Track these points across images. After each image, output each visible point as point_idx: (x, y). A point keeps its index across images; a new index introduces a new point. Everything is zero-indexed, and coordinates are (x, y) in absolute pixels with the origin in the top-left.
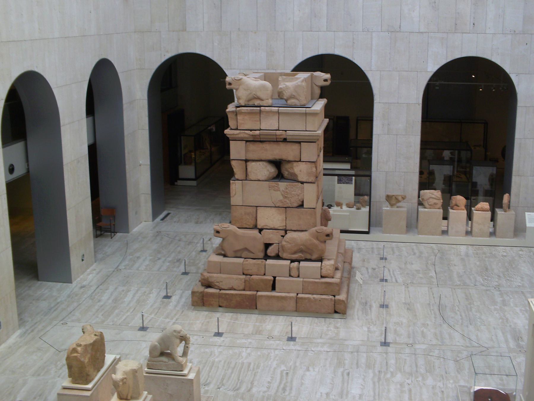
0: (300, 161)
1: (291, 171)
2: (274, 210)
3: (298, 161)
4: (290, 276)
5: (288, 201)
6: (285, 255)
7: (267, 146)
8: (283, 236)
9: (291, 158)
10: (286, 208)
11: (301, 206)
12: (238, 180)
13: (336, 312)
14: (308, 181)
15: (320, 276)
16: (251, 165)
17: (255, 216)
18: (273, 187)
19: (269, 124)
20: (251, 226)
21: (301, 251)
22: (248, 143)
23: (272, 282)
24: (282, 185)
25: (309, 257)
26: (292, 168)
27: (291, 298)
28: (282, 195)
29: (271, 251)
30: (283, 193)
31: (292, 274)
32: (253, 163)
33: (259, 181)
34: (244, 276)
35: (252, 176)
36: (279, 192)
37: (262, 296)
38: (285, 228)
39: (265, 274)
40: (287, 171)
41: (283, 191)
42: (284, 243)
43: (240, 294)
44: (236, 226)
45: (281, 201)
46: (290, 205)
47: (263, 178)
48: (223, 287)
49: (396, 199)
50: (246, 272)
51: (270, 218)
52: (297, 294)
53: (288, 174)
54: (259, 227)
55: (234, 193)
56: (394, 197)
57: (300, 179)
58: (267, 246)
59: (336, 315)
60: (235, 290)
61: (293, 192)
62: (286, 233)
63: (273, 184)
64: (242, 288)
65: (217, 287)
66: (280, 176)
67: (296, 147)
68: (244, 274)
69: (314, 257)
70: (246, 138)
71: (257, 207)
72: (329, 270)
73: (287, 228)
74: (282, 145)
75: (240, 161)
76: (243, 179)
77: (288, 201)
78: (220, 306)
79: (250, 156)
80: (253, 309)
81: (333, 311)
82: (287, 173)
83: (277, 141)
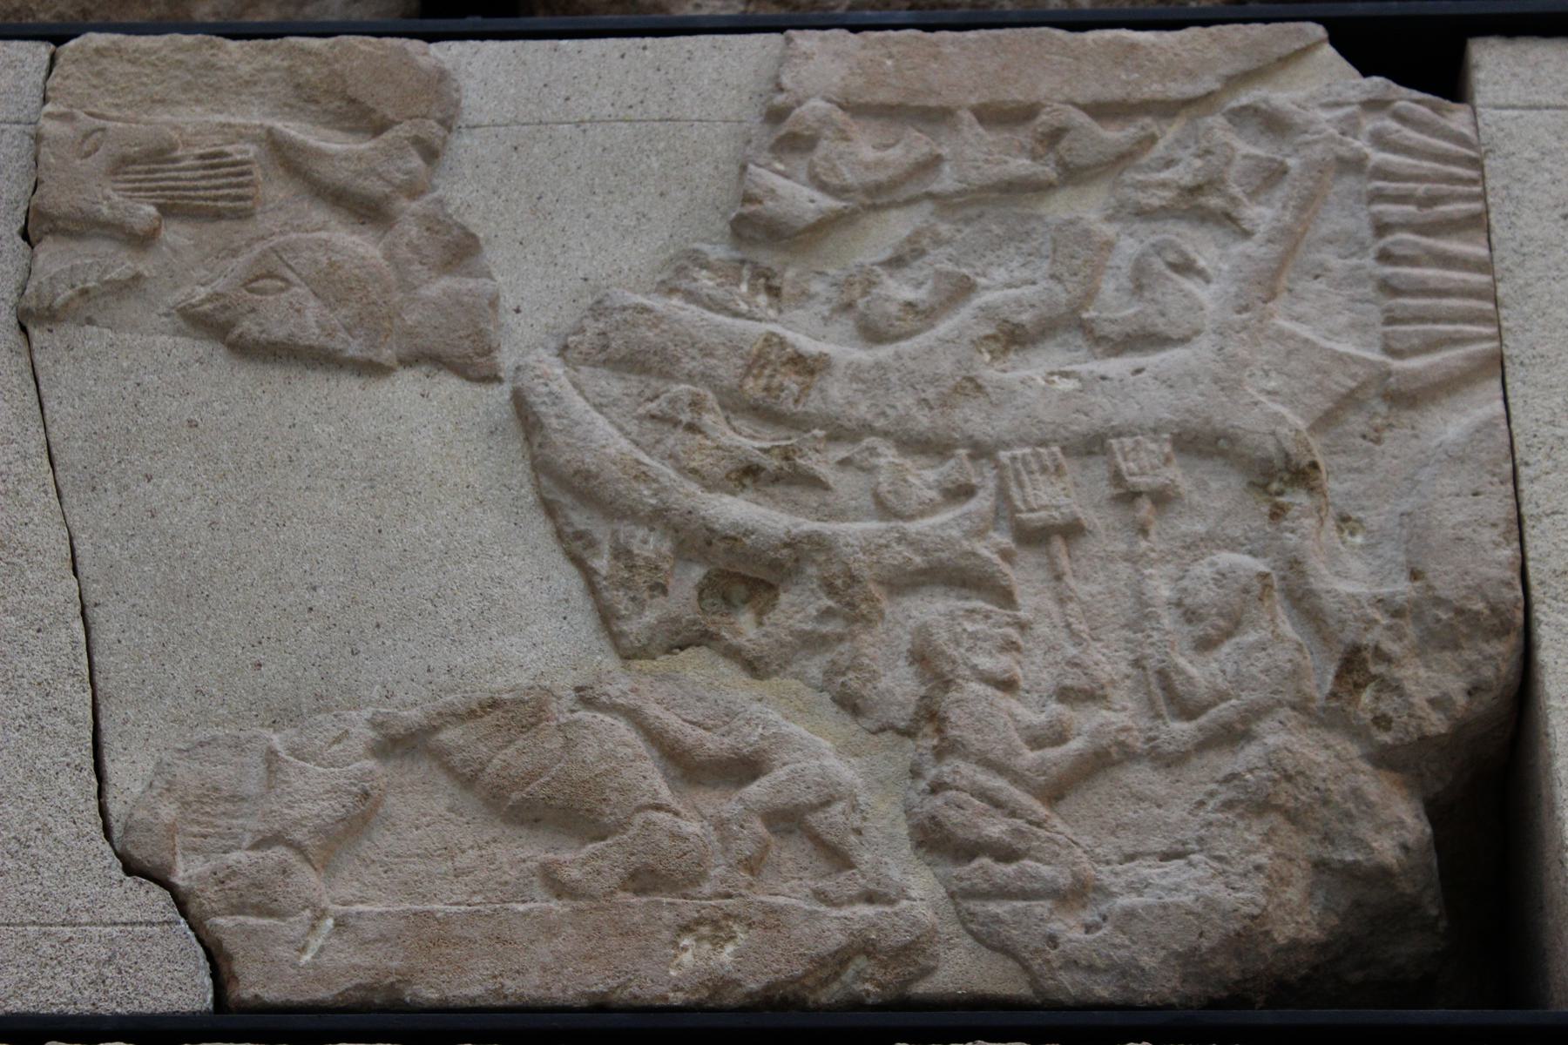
18: (206, 195)
28: (569, 496)
41: (623, 353)
61: (1042, 381)
77: (814, 750)
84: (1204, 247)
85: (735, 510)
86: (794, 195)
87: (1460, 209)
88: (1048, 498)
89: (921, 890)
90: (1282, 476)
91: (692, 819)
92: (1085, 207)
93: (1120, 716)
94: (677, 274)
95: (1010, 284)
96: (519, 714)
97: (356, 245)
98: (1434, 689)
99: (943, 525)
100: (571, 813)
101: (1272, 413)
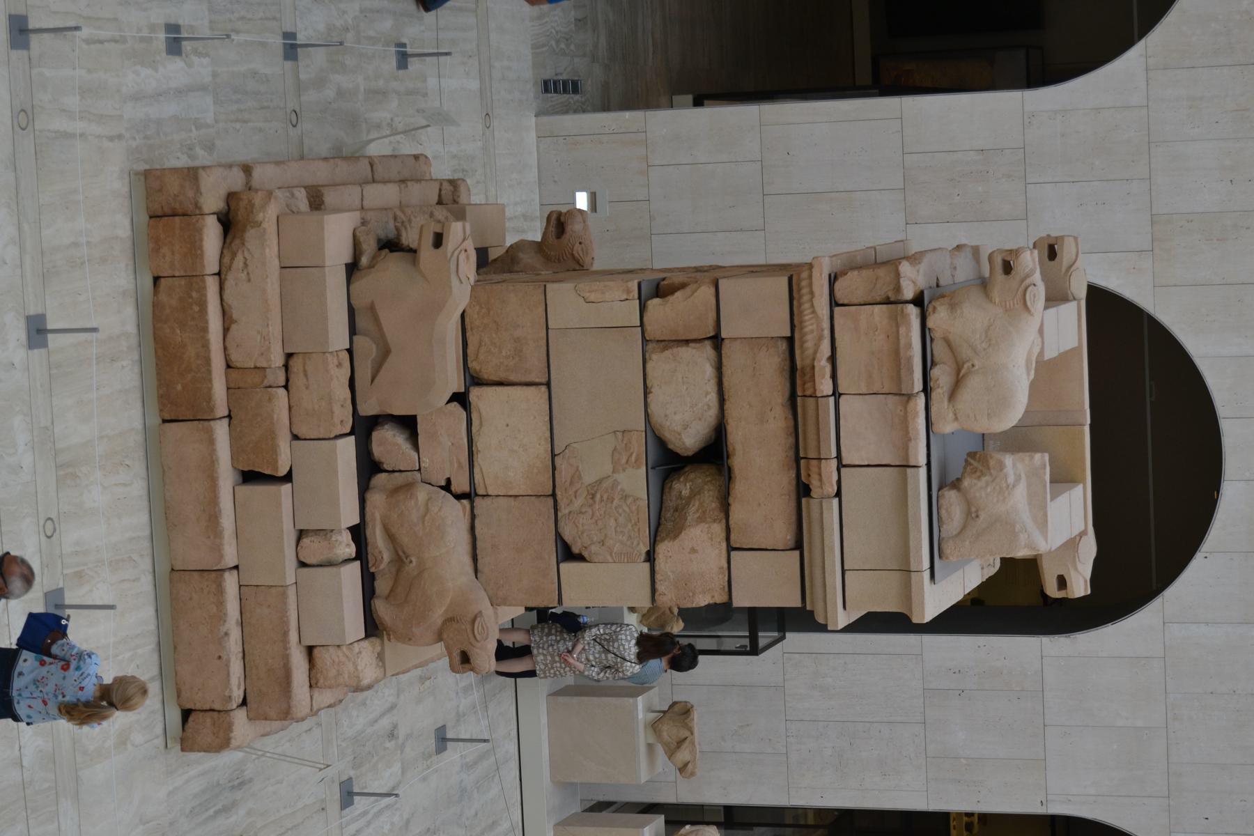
0: (731, 549)
1: (692, 512)
2: (543, 449)
3: (728, 539)
4: (301, 534)
5: (578, 503)
6: (376, 499)
7: (778, 421)
8: (447, 487)
10: (554, 495)
11: (568, 554)
12: (643, 309)
13: (186, 714)
14: (658, 577)
16: (702, 357)
17: (513, 378)
19: (860, 428)
20: (473, 365)
21: (400, 560)
22: (783, 346)
23: (268, 472)
24: (636, 481)
25: (382, 586)
26: (701, 520)
27: (218, 549)
28: (600, 481)
29: (388, 442)
30: (605, 485)
31: (306, 541)
32: (709, 371)
33: (646, 391)
34: (278, 361)
35: (660, 363)
36: (608, 468)
37: (211, 441)
38: (481, 491)
39: (296, 437)
40: (694, 494)
42: (422, 493)
43: (208, 361)
44: (470, 305)
45: (576, 476)
46: (564, 511)
47: (654, 408)
48: (229, 284)
49: (680, 742)
50: (296, 364)
51: (510, 435)
52: (236, 567)
53: (680, 497)
54: (475, 394)
55: (592, 297)
56: (685, 733)
57: (663, 549)
58: (409, 424)
59: (175, 716)
60: (226, 330)
61: (612, 523)
62: (459, 497)
64: (236, 358)
65: (226, 260)
66: (669, 463)
67: (782, 532)
68: (289, 356)
69: (382, 609)
71: (548, 384)
72: (339, 674)
73: (478, 501)
74: (783, 481)
75: (712, 315)
76: (648, 328)
77: (578, 503)
78: (156, 279)
79: (735, 357)
80: (161, 410)
81: (188, 706)
82: (686, 492)
83: (797, 459)
84: (625, 538)
85: (598, 496)
86: (630, 500)
87: (631, 560)
88: (600, 523)
89: (567, 511)
90: (602, 543)
91: (571, 492)
92: (630, 526)
93: (581, 528)
94: (622, 490)
95: (621, 520)
96: (580, 477)
97: (624, 461)
98: (585, 554)
99: (598, 514)
100: (571, 483)
101: (609, 542)
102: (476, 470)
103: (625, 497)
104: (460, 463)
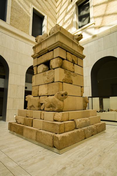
9: (50, 59)
14: (56, 67)
15: (52, 120)
29: (42, 107)
36: (46, 77)
54: (39, 95)
63: (44, 73)
67: (52, 52)
70: (37, 56)
77: (49, 80)
102: (46, 95)
103: (48, 74)
104: (45, 97)
